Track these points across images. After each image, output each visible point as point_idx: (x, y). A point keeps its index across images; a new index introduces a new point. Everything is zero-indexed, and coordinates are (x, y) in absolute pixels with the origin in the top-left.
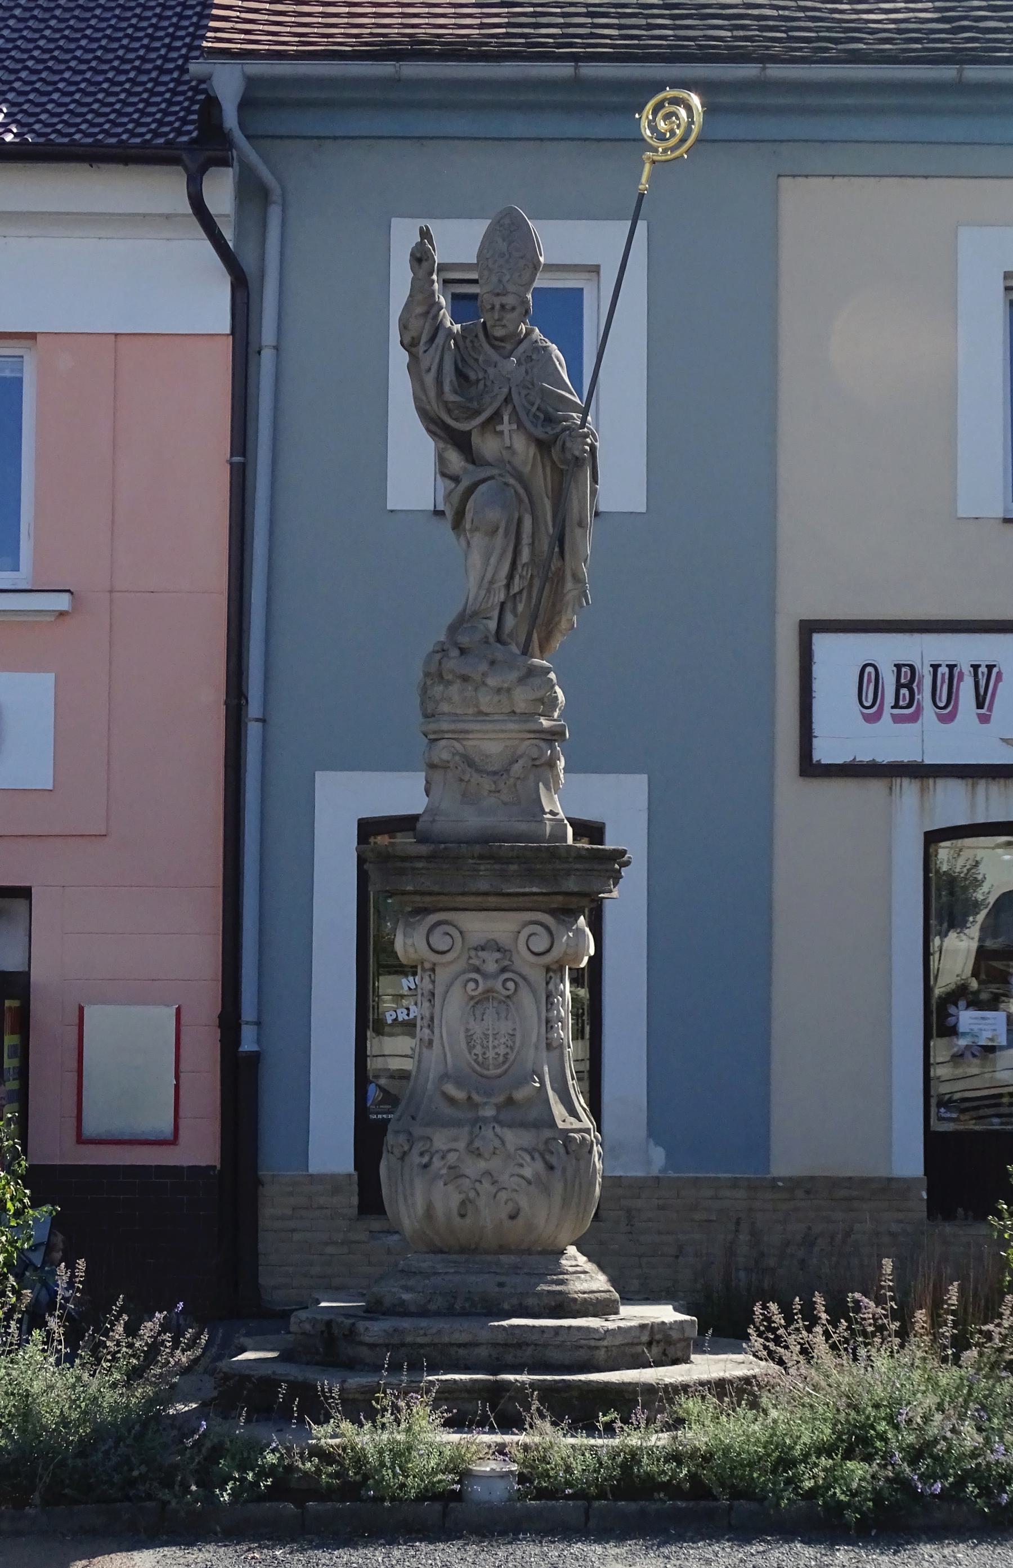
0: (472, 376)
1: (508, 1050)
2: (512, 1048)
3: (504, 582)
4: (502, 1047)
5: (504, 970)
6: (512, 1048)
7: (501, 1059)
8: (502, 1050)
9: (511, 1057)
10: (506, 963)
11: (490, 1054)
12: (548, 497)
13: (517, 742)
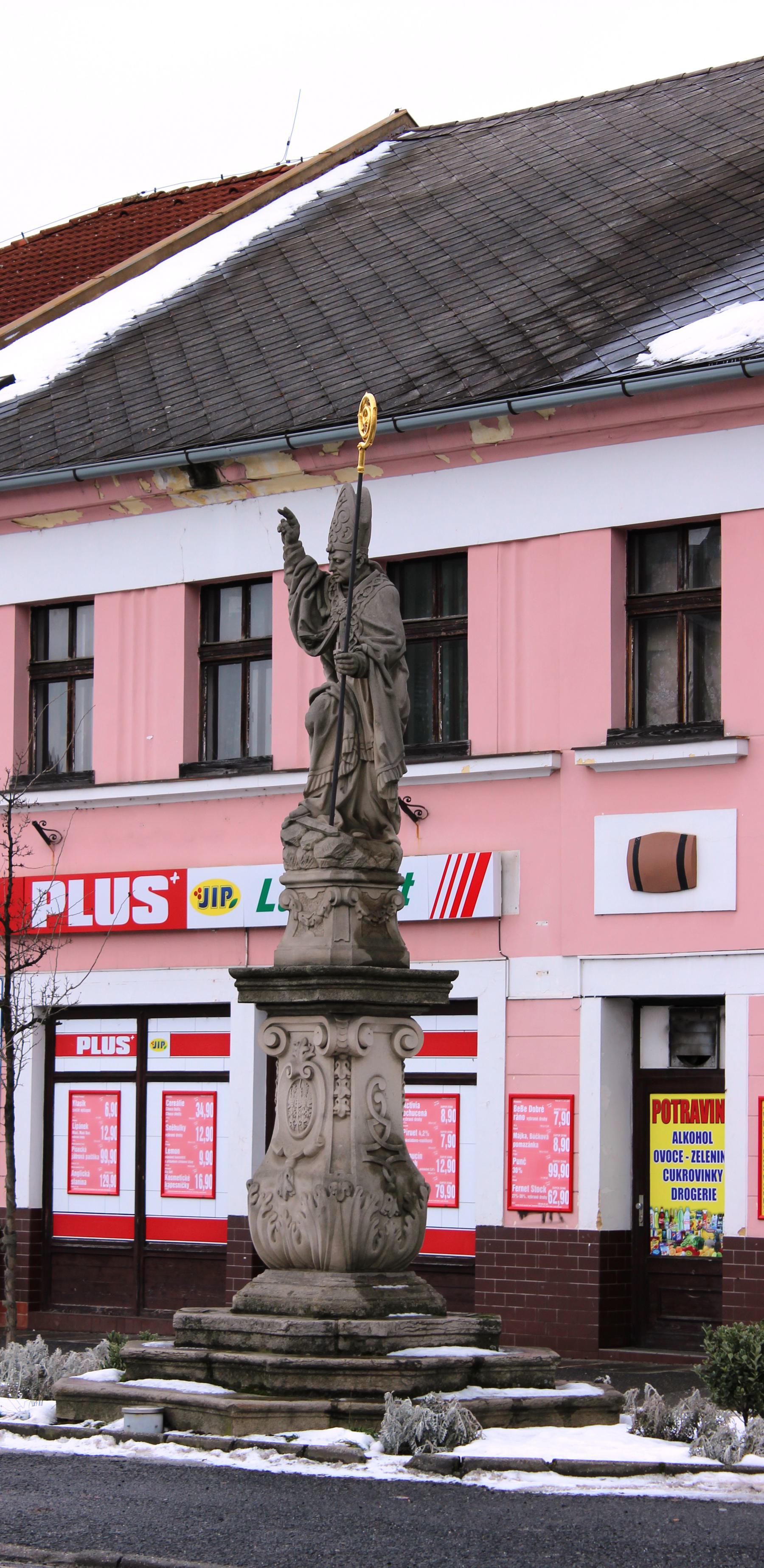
0: (323, 613)
1: (306, 1119)
2: (309, 1117)
3: (329, 768)
4: (303, 1117)
5: (309, 1059)
6: (309, 1117)
7: (303, 1126)
8: (303, 1119)
9: (309, 1125)
10: (310, 1054)
11: (297, 1123)
12: (365, 700)
13: (322, 890)
